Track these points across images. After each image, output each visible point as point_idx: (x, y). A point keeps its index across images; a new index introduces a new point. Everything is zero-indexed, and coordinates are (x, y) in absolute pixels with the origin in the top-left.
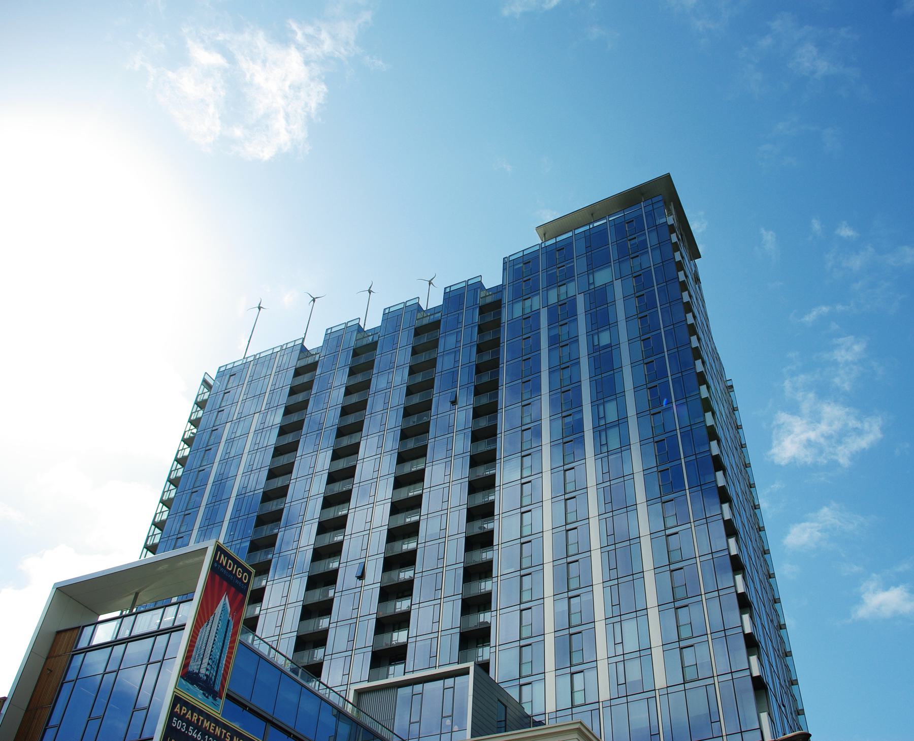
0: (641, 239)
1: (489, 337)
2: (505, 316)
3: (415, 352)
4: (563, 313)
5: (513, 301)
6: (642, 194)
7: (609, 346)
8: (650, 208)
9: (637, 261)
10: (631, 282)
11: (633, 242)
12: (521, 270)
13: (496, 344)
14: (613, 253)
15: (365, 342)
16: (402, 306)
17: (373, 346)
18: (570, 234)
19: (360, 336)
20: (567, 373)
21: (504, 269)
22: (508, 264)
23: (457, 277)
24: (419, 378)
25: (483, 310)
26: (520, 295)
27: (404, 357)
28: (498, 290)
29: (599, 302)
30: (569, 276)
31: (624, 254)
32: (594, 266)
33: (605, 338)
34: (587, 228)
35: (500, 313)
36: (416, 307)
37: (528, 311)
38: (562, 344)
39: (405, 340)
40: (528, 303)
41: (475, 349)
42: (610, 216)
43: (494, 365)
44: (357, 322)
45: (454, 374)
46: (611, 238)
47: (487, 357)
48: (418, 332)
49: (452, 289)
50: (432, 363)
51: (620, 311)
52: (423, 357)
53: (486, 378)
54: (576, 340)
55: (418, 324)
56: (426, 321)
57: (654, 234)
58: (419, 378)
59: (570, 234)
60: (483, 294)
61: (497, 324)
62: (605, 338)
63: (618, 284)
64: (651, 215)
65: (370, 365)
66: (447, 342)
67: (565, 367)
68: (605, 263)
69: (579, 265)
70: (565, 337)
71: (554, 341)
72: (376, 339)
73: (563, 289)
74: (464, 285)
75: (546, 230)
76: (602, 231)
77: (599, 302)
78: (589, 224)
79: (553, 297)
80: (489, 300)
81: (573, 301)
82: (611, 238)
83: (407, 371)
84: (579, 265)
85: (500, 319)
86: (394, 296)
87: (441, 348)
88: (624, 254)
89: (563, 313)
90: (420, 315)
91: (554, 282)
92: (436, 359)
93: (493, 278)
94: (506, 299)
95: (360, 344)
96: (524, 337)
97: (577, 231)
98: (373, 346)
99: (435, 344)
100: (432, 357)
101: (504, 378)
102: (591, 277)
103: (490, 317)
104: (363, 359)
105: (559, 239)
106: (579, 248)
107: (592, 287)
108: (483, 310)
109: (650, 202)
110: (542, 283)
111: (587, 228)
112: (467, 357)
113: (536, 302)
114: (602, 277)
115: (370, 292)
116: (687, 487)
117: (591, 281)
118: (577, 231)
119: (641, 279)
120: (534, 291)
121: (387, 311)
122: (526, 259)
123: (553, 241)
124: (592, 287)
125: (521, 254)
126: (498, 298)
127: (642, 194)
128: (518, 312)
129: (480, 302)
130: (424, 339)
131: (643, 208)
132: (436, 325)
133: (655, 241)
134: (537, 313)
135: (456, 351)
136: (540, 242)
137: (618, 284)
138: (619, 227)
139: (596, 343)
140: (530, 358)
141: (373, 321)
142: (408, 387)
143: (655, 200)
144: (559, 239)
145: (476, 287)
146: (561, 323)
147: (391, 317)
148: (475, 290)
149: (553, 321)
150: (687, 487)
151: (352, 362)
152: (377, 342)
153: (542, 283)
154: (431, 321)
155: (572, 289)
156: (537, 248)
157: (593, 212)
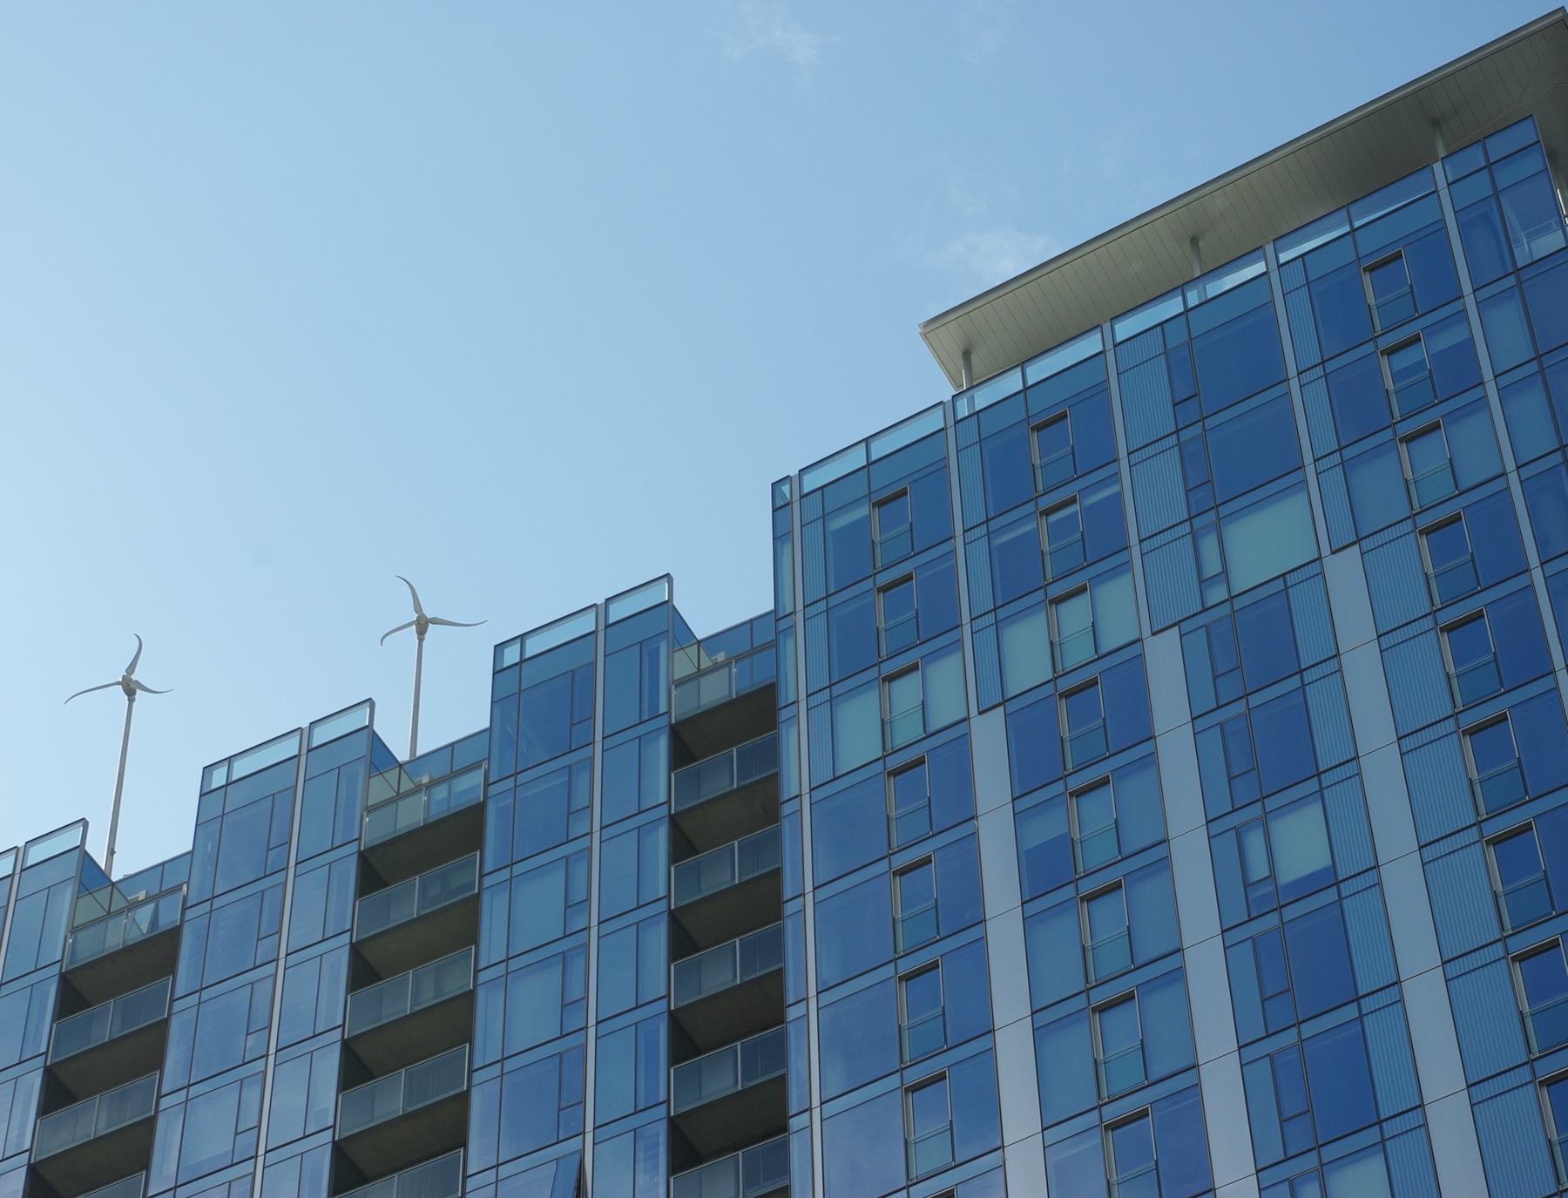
0: (1444, 341)
1: (724, 872)
2: (798, 763)
3: (364, 971)
4: (1083, 731)
5: (833, 691)
6: (1436, 123)
7: (1327, 879)
8: (1480, 186)
9: (1432, 452)
10: (1411, 558)
11: (1405, 359)
12: (869, 537)
13: (760, 906)
14: (1310, 417)
15: (116, 936)
16: (290, 748)
17: (158, 954)
18: (1090, 345)
19: (90, 909)
20: (1123, 1026)
21: (780, 537)
22: (796, 509)
23: (551, 584)
24: (392, 1099)
25: (689, 743)
26: (866, 661)
27: (311, 992)
28: (756, 640)
29: (1259, 652)
30: (1101, 550)
31: (1364, 425)
32: (1214, 498)
33: (1300, 844)
34: (1174, 306)
35: (771, 754)
36: (360, 747)
37: (908, 730)
38: (1087, 886)
39: (318, 912)
40: (906, 692)
41: (658, 939)
42: (1280, 240)
43: (759, 1011)
44: (71, 840)
45: (566, 1065)
46: (1296, 343)
47: (722, 973)
48: (376, 871)
49: (534, 647)
50: (453, 1023)
51: (1368, 702)
52: (406, 995)
53: (723, 1078)
54: (1155, 859)
55: (375, 831)
56: (411, 815)
57: (1509, 317)
58: (392, 1099)
59: (1090, 345)
60: (684, 665)
61: (762, 806)
62: (1300, 844)
63: (1345, 572)
64: (1484, 220)
65: (144, 1053)
66: (516, 915)
67: (1115, 993)
68: (1275, 474)
69: (1149, 491)
70: (1098, 851)
71: (1049, 876)
72: (169, 917)
73: (1075, 614)
74: (586, 624)
75: (967, 335)
76: (1251, 321)
77: (1259, 652)
78: (1181, 288)
79: (1028, 656)
80: (715, 691)
81: (1128, 667)
82: (1296, 343)
83: (329, 1065)
84: (1149, 491)
85: (774, 780)
86: (247, 698)
87: (492, 943)
88: (1364, 425)
89: (1083, 731)
90: (380, 789)
91: (1025, 585)
92: (469, 998)
93: (727, 584)
94: (796, 683)
95: (91, 947)
96: (900, 861)
97: (1126, 328)
98: (158, 954)
99: (459, 927)
100: (454, 986)
101: (810, 1068)
102: (1209, 545)
103: (723, 776)
104: (106, 1023)
105: (1039, 371)
106: (1142, 408)
107: (1217, 594)
108: (689, 743)
109: (1475, 157)
110: (972, 583)
111: (1174, 306)
112: (632, 975)
113: (946, 688)
114: (1264, 543)
115: (130, 688)
116: (1467, 288)
117: (1212, 566)
118: (1126, 328)
119: (1462, 544)
120: (934, 632)
121: (219, 778)
122: (883, 480)
123: (1011, 383)
124: (1217, 594)
125: (857, 460)
126: (760, 680)
127: (1436, 123)
128: (859, 742)
129: (679, 706)
130: (409, 901)
131: (1443, 189)
132: (460, 832)
133: (1517, 347)
134: (954, 746)
135: (564, 954)
136: (947, 393)
137: (1345, 572)
138: (1328, 289)
139: (1259, 870)
140: (934, 960)
141: (152, 833)
142: (338, 1148)
143: (1499, 146)
144: (1039, 371)
145: (650, 628)
146: (1075, 782)
147: (241, 808)
148: (647, 651)
149: (1033, 778)
150: (1467, 288)
151: (58, 1039)
152: (175, 934)
153: (972, 583)
154: (437, 812)
155: (1117, 609)
156: (934, 422)
157: (1198, 228)
